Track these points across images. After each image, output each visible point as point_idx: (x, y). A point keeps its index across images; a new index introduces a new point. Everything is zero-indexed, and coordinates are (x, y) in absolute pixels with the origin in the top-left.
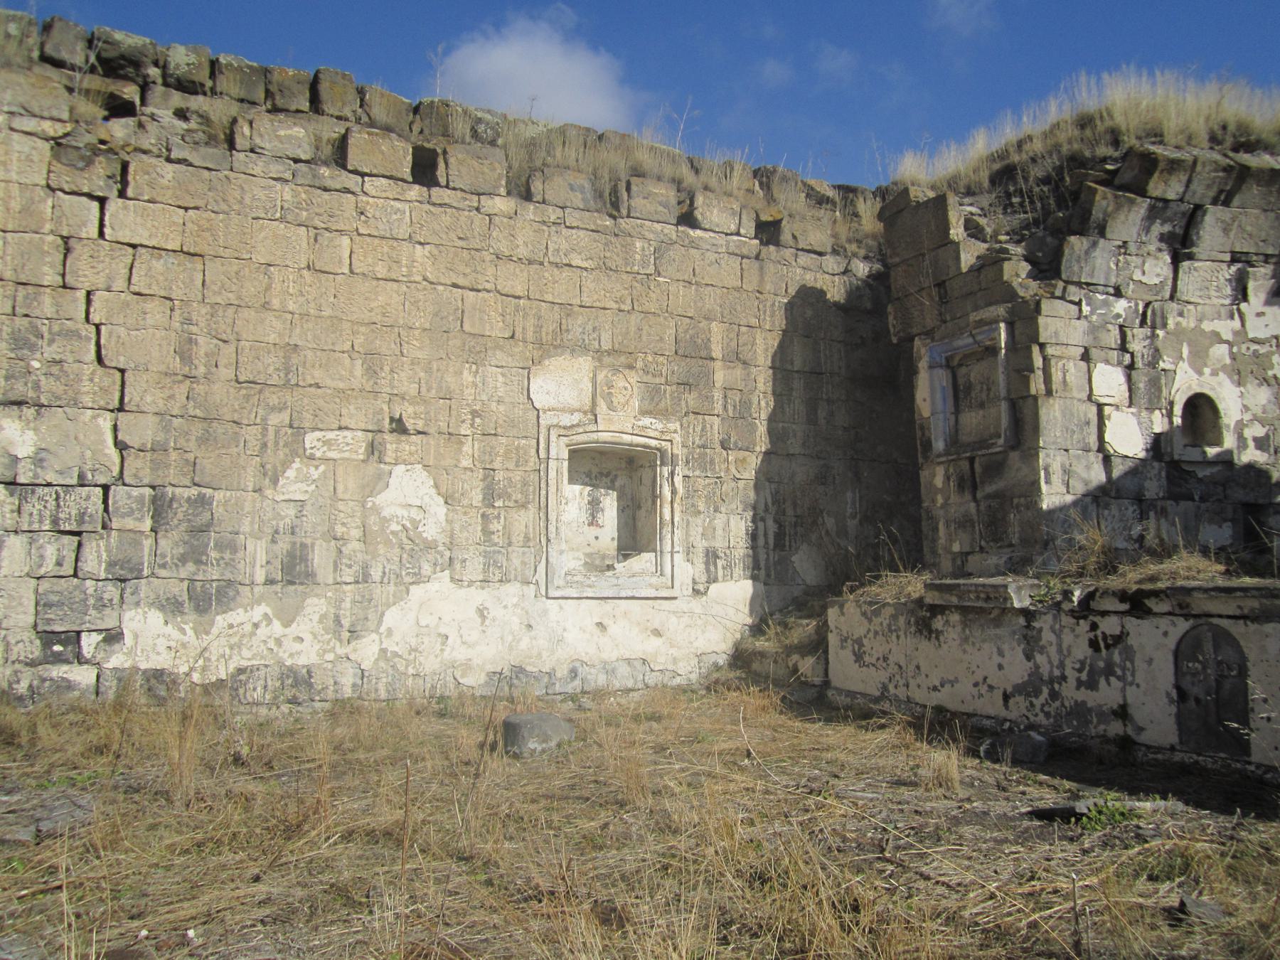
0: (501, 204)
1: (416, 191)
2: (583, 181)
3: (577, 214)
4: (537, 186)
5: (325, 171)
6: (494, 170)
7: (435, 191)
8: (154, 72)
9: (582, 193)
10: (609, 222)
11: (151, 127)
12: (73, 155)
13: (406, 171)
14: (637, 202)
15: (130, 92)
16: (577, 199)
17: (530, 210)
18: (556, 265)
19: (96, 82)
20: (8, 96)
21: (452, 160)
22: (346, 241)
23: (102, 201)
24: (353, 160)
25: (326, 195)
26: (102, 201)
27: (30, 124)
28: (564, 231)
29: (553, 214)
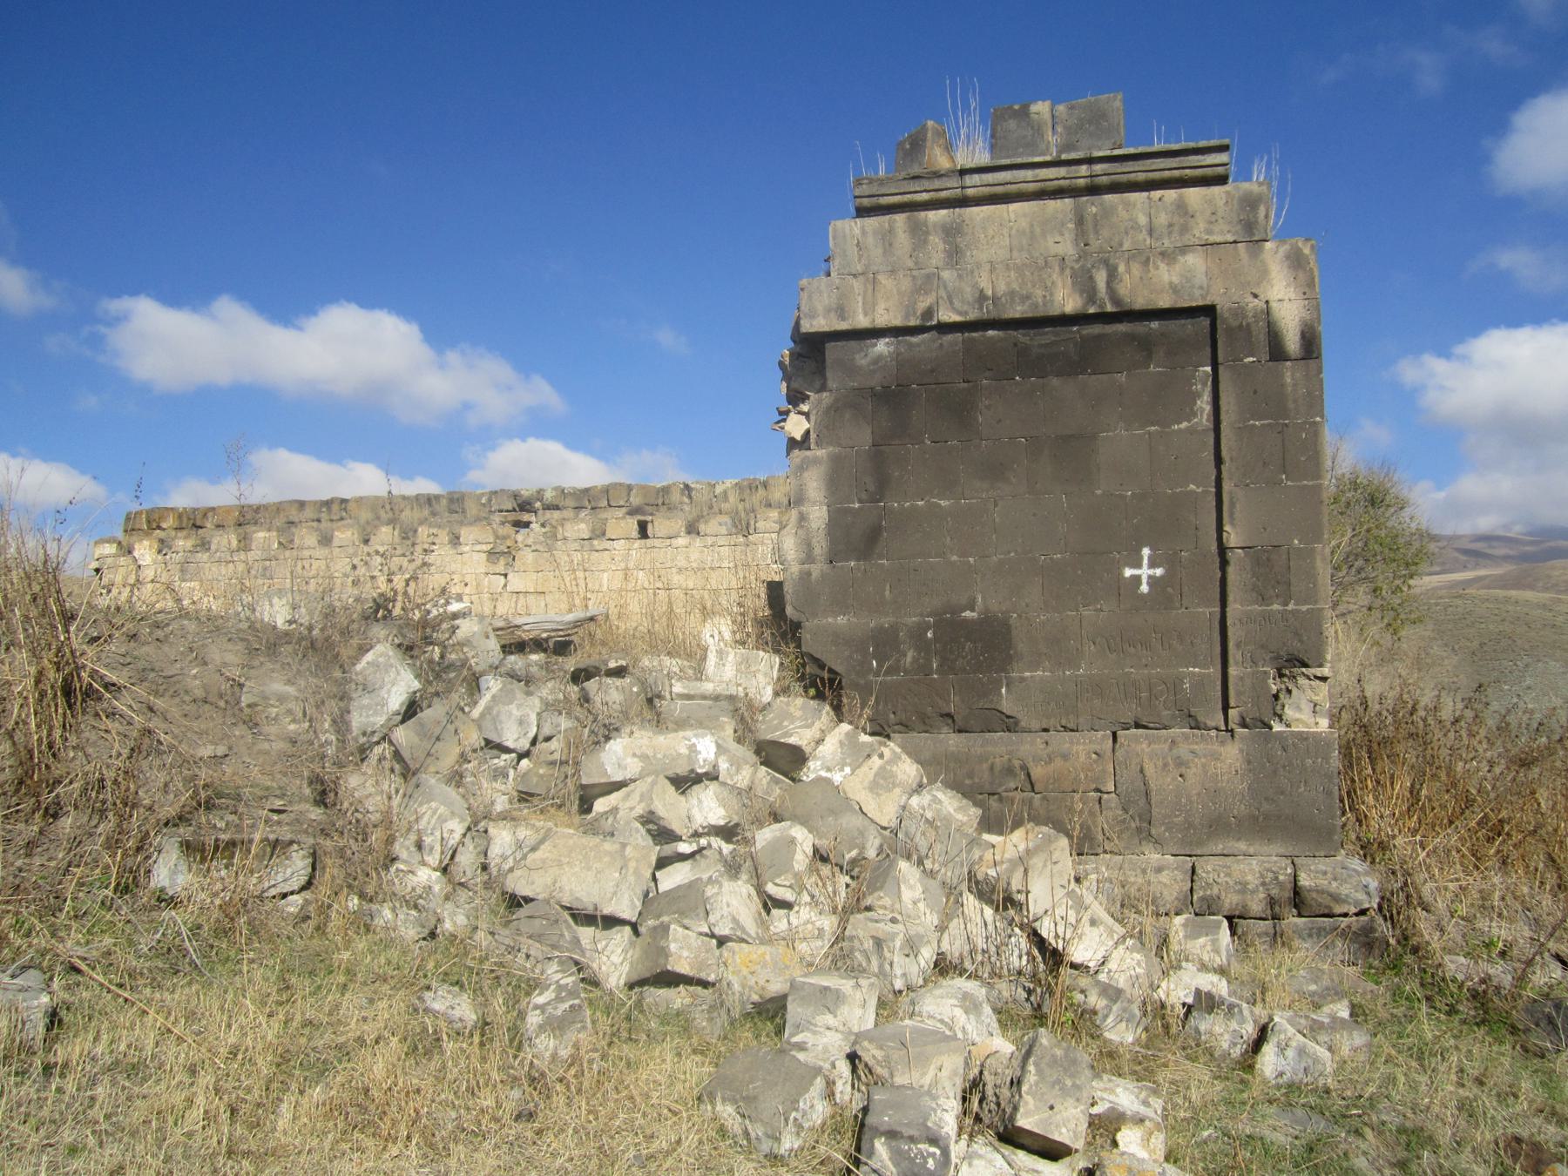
0: (682, 541)
1: (638, 544)
2: (726, 519)
3: (724, 538)
4: (702, 527)
5: (595, 542)
6: (678, 524)
7: (648, 542)
8: (538, 505)
9: (726, 524)
10: (741, 539)
11: (532, 534)
12: (493, 557)
13: (635, 533)
14: (760, 525)
15: (526, 517)
16: (723, 530)
17: (698, 542)
18: (712, 569)
19: (512, 517)
20: (471, 537)
21: (656, 523)
22: (606, 575)
23: (506, 575)
24: (608, 535)
25: (596, 554)
26: (506, 575)
27: (478, 547)
28: (717, 549)
29: (710, 540)
